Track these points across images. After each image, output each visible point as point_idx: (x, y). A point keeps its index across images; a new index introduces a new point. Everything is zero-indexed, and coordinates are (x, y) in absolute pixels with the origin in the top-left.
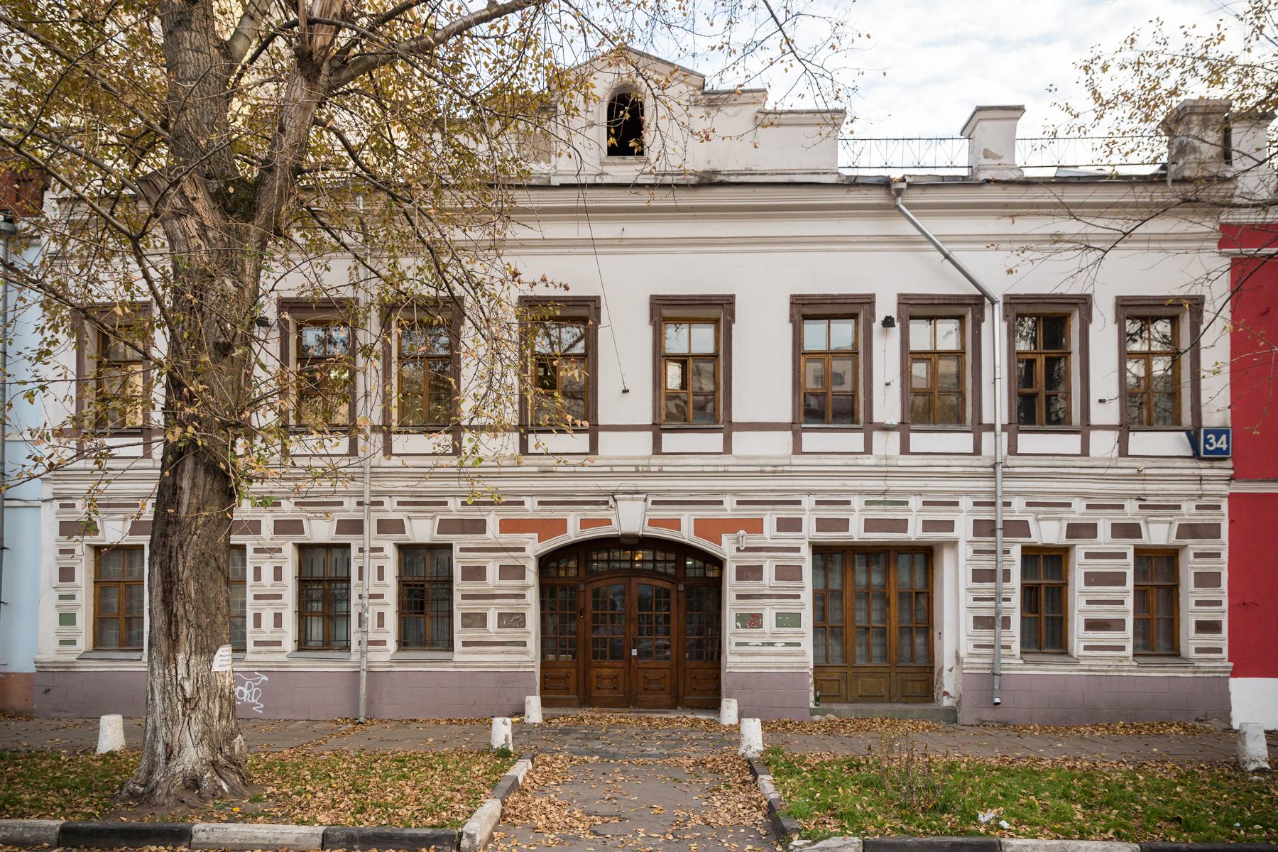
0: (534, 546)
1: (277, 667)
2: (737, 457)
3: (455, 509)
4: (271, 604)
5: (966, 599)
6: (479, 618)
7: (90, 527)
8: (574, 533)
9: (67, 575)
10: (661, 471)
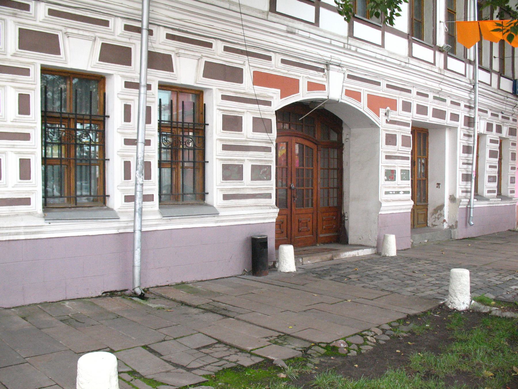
1: (26, 233)
2: (388, 52)
6: (236, 169)
10: (356, 51)
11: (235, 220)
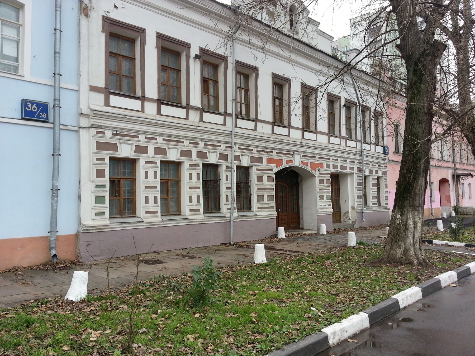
0: (276, 170)
2: (319, 142)
3: (255, 153)
4: (195, 191)
5: (356, 191)
6: (262, 197)
7: (114, 147)
8: (285, 165)
9: (100, 173)
11: (262, 217)
